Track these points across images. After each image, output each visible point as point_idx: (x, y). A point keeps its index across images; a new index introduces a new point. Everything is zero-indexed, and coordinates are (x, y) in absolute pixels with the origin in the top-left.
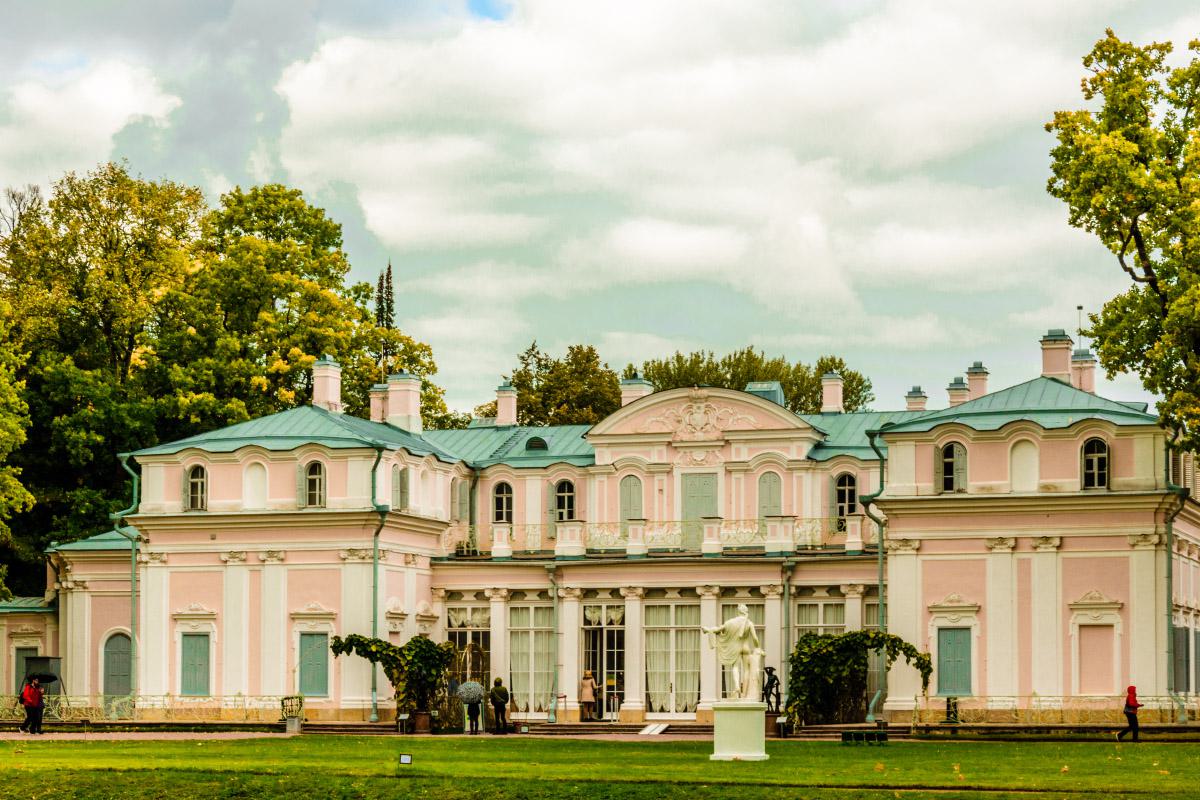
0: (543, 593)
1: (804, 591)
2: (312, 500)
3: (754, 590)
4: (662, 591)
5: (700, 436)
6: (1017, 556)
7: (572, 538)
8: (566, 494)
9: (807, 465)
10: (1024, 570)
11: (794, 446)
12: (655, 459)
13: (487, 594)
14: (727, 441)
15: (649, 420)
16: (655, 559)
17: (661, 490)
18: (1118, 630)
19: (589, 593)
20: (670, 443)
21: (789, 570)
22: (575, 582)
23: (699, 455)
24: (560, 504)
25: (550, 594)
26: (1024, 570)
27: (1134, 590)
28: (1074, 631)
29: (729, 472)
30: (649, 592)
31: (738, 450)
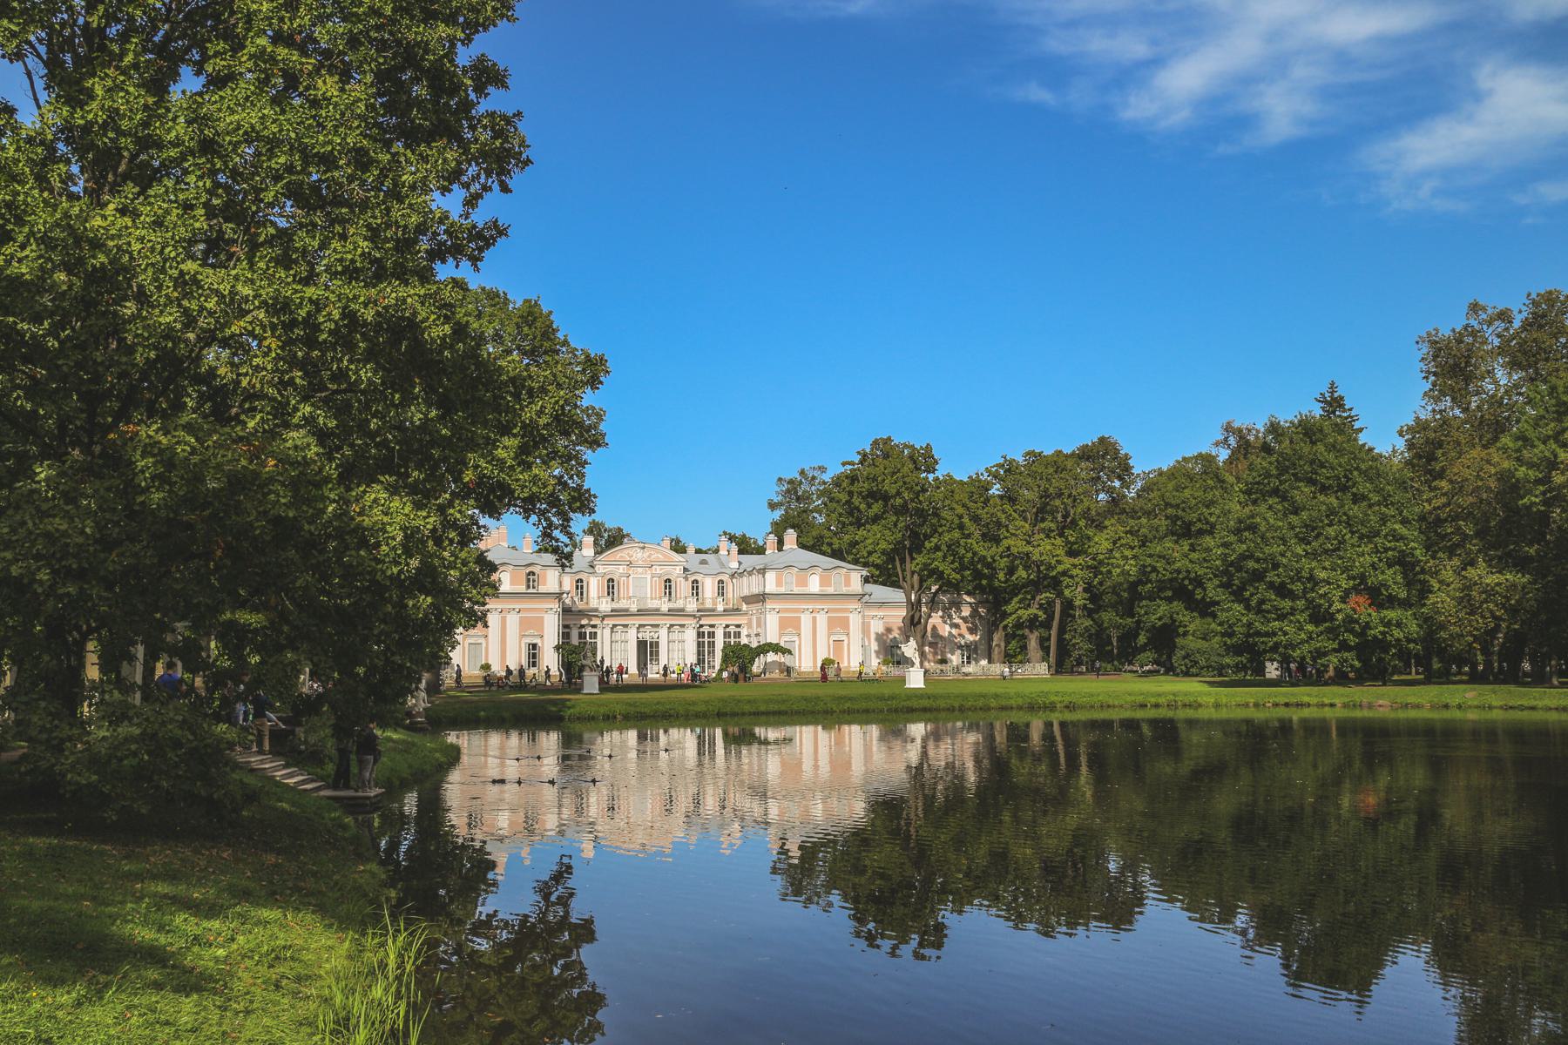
1: (701, 626)
2: (528, 587)
3: (682, 626)
4: (644, 626)
5: (640, 562)
6: (813, 615)
10: (814, 619)
11: (678, 568)
12: (621, 571)
16: (642, 613)
18: (846, 642)
21: (694, 616)
22: (610, 622)
23: (640, 570)
26: (814, 619)
27: (851, 628)
28: (831, 642)
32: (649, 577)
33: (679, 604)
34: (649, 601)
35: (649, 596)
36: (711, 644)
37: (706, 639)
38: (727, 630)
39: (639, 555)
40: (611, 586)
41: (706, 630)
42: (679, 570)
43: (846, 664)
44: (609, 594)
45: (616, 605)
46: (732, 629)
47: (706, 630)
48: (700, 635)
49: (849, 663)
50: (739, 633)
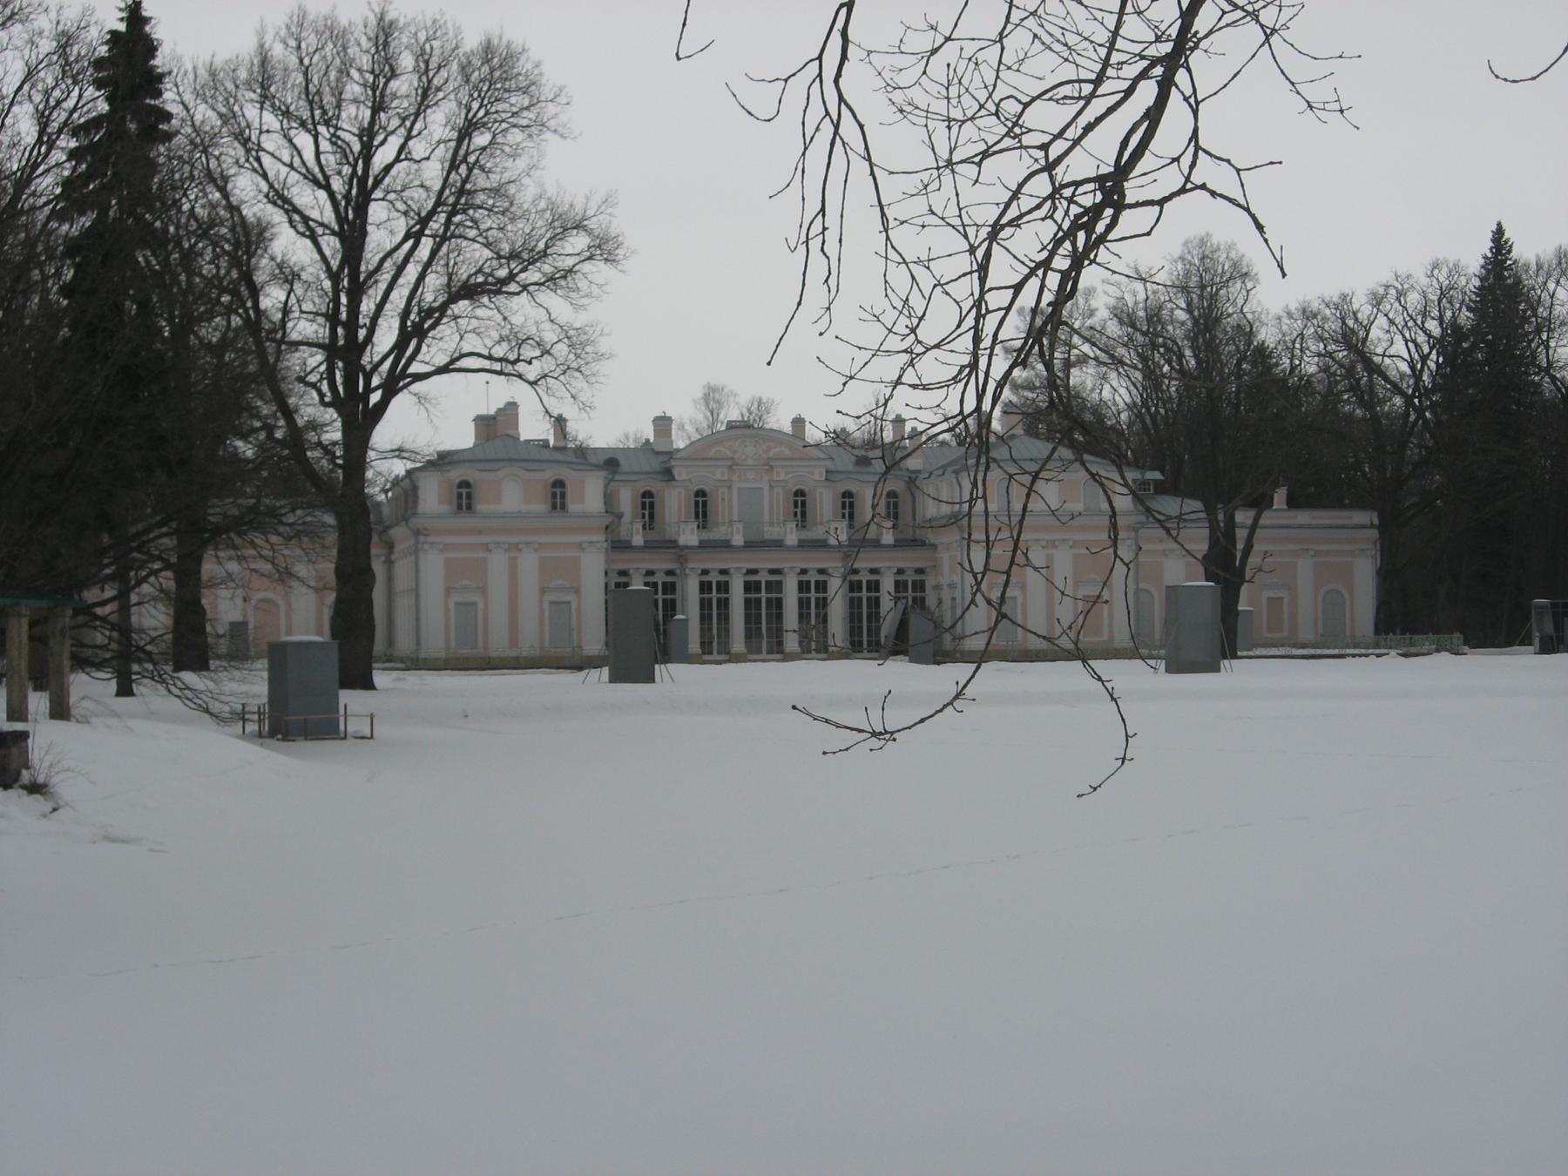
0: (670, 573)
5: (750, 462)
7: (692, 533)
8: (647, 500)
9: (827, 484)
12: (718, 476)
13: (631, 572)
14: (772, 467)
15: (713, 450)
17: (723, 499)
19: (705, 572)
20: (730, 467)
23: (751, 475)
24: (644, 506)
25: (678, 572)
29: (771, 487)
30: (751, 572)
31: (778, 474)
32: (766, 488)
33: (816, 533)
34: (766, 528)
35: (766, 518)
36: (875, 603)
37: (864, 594)
38: (900, 578)
39: (750, 449)
40: (701, 508)
41: (864, 577)
42: (819, 475)
43: (1105, 638)
44: (697, 517)
45: (706, 536)
46: (910, 577)
47: (864, 577)
48: (855, 587)
49: (1111, 632)
50: (922, 583)
